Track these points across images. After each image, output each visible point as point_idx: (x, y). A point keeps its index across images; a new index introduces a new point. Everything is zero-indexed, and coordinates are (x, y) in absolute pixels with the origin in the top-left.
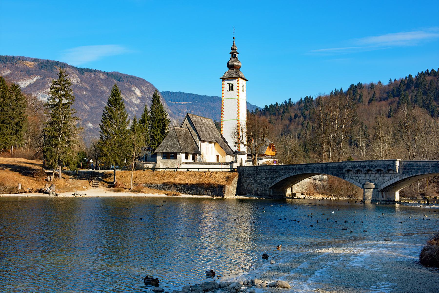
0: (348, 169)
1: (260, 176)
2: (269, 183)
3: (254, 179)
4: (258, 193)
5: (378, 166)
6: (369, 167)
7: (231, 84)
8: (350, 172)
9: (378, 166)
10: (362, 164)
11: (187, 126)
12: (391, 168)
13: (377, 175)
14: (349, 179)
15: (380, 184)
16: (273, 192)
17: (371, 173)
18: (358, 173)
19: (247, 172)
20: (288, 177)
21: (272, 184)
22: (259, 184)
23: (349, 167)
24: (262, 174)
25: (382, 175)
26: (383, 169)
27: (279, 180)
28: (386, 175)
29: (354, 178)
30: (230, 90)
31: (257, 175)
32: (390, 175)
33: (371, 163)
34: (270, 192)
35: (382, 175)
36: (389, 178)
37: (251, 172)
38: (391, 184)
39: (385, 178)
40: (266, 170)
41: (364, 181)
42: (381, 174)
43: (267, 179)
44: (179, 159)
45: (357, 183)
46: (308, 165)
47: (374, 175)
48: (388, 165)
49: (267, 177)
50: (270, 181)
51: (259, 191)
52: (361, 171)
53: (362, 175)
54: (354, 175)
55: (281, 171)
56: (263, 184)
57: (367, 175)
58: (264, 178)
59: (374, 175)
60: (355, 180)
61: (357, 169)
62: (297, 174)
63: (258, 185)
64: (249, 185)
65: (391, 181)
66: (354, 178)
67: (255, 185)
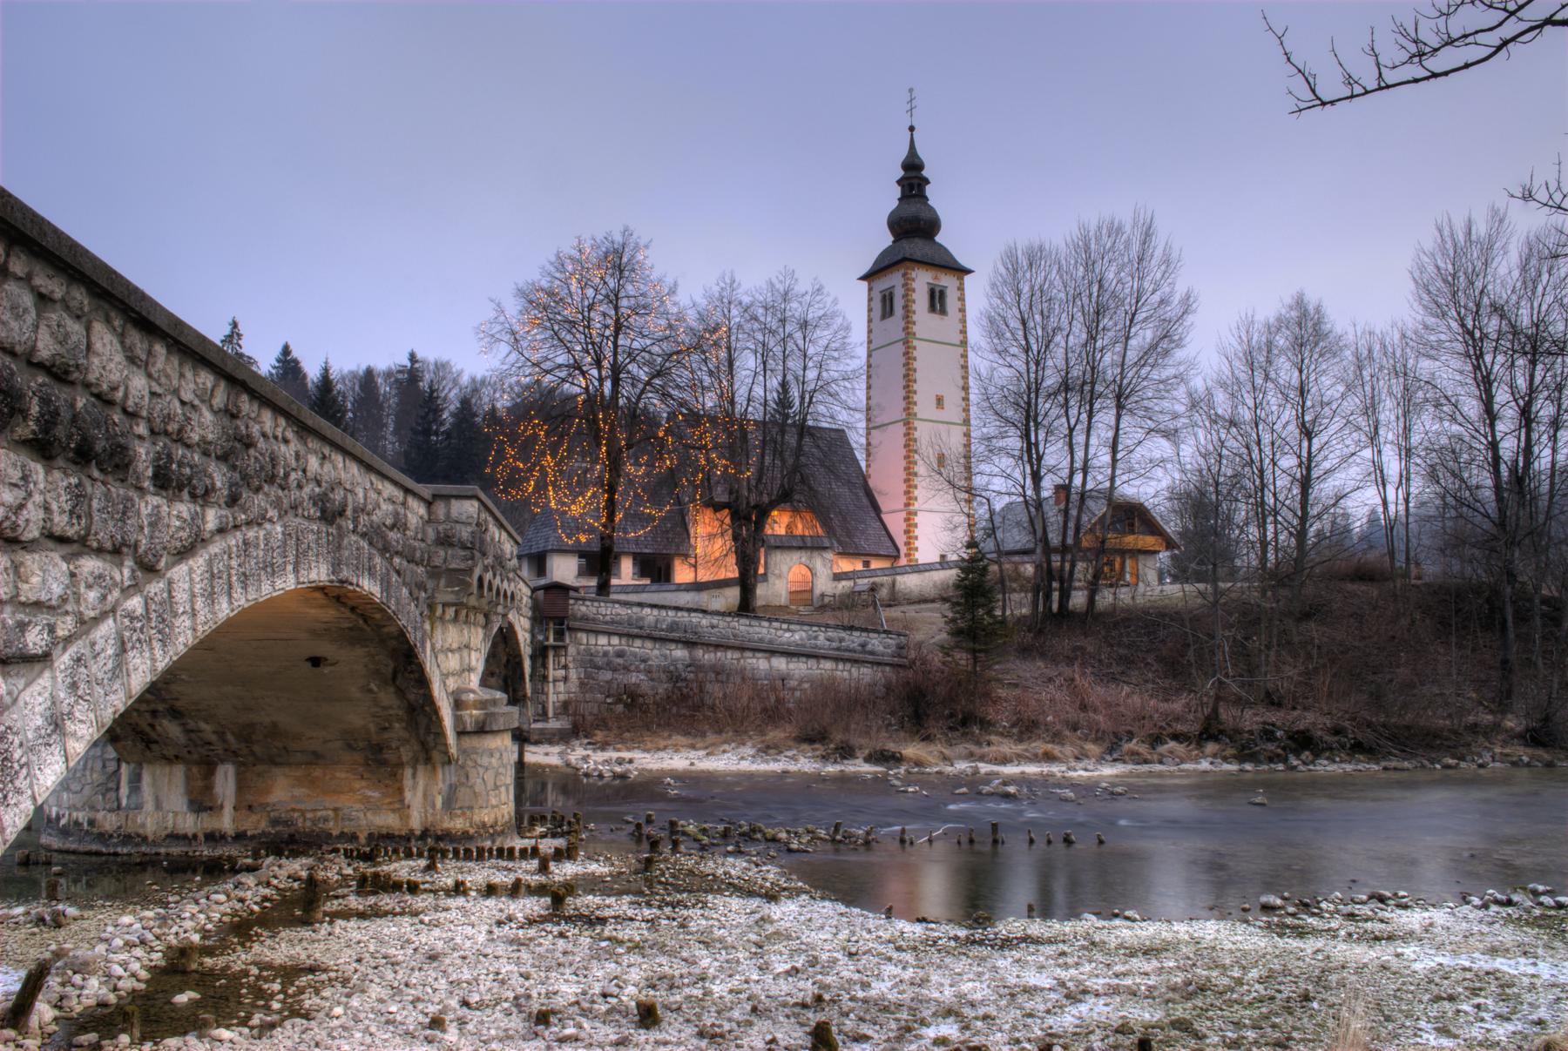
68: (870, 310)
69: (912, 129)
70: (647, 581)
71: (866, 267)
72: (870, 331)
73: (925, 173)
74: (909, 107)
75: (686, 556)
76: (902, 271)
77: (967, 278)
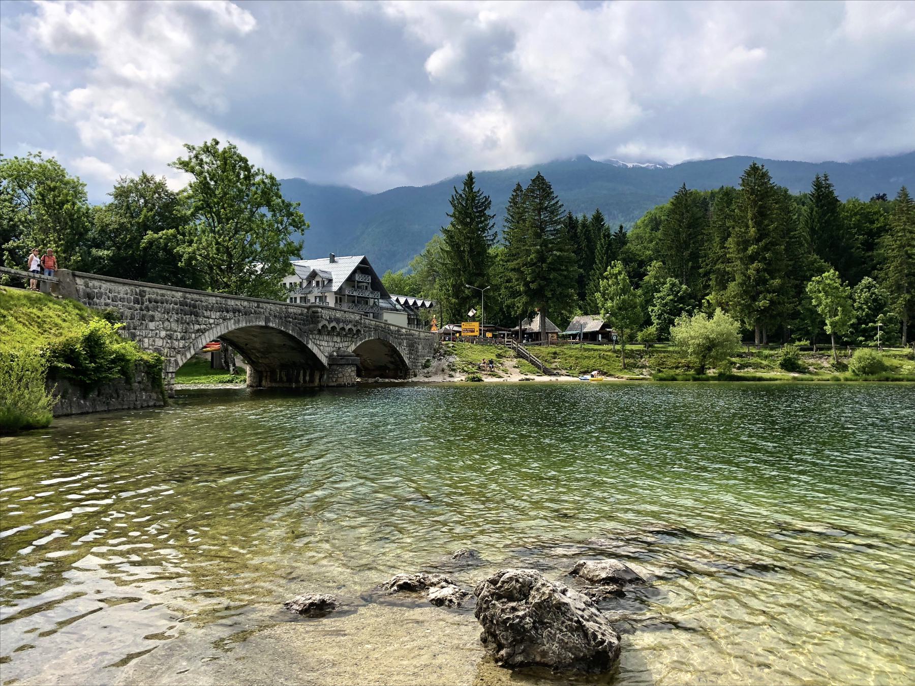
1: (152, 325)
2: (178, 352)
21: (186, 357)
24: (157, 315)
31: (143, 318)
43: (170, 337)
58: (163, 334)
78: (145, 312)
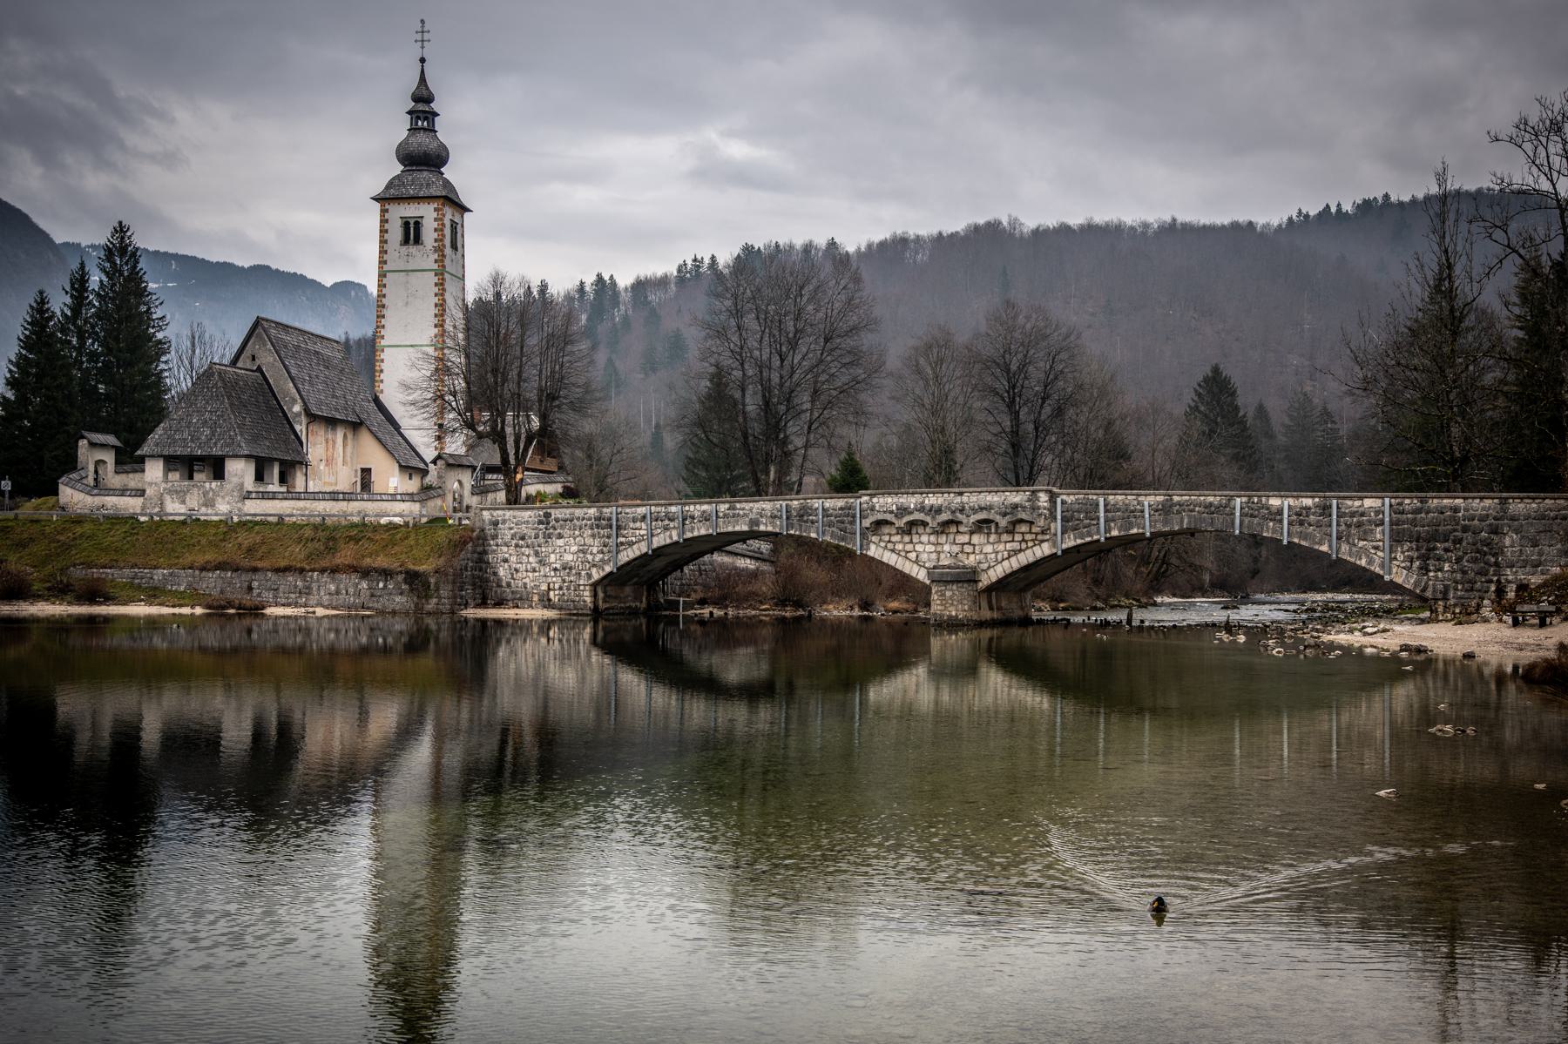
0: (880, 517)
1: (560, 542)
2: (594, 566)
3: (537, 554)
4: (549, 600)
5: (982, 509)
6: (953, 512)
7: (412, 222)
8: (886, 530)
9: (982, 509)
10: (927, 502)
11: (258, 362)
12: (1023, 516)
13: (976, 539)
14: (882, 550)
15: (985, 566)
16: (607, 598)
17: (958, 532)
18: (914, 531)
19: (511, 529)
20: (663, 543)
21: (603, 570)
22: (555, 569)
23: (885, 512)
25: (993, 538)
26: (998, 518)
27: (632, 556)
28: (1005, 537)
29: (899, 547)
30: (406, 241)
31: (548, 536)
32: (1018, 537)
33: (958, 499)
34: (595, 595)
35: (993, 538)
36: (1016, 546)
37: (524, 529)
38: (1022, 565)
39: (1001, 547)
40: (583, 519)
41: (934, 556)
42: (989, 534)
44: (235, 480)
45: (907, 562)
46: (738, 506)
47: (965, 538)
48: (1015, 506)
49: (585, 545)
50: (597, 559)
51: (557, 592)
52: (925, 524)
53: (925, 538)
54: (899, 536)
55: (638, 525)
56: (571, 568)
57: (943, 539)
58: (574, 548)
59: (965, 538)
60: (903, 554)
61: (911, 518)
62: (696, 534)
63: (552, 573)
64: (517, 571)
65: (1021, 556)
66: (899, 547)
67: (542, 573)
68: (383, 231)
69: (423, 60)
70: (284, 489)
71: (378, 187)
72: (383, 252)
73: (435, 106)
74: (419, 37)
75: (301, 463)
76: (436, 205)
77: (467, 215)
78: (551, 531)
